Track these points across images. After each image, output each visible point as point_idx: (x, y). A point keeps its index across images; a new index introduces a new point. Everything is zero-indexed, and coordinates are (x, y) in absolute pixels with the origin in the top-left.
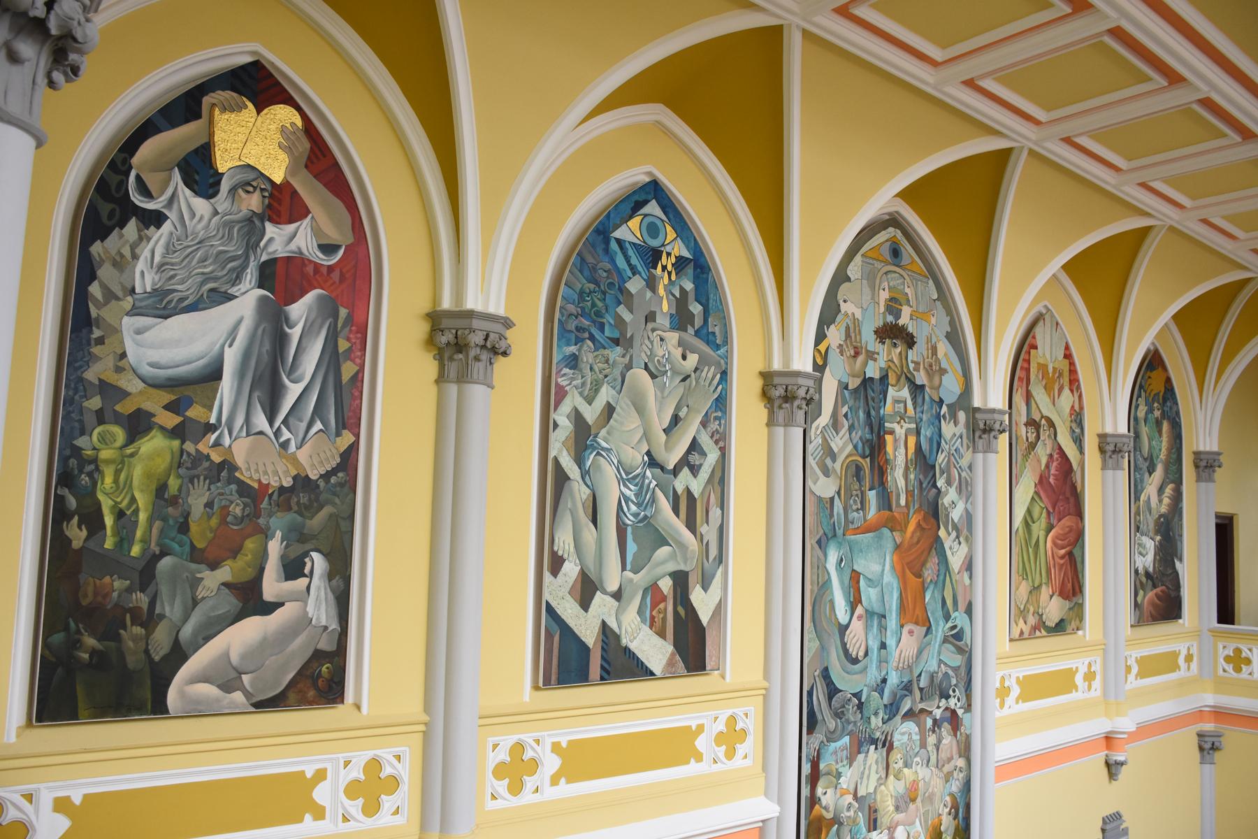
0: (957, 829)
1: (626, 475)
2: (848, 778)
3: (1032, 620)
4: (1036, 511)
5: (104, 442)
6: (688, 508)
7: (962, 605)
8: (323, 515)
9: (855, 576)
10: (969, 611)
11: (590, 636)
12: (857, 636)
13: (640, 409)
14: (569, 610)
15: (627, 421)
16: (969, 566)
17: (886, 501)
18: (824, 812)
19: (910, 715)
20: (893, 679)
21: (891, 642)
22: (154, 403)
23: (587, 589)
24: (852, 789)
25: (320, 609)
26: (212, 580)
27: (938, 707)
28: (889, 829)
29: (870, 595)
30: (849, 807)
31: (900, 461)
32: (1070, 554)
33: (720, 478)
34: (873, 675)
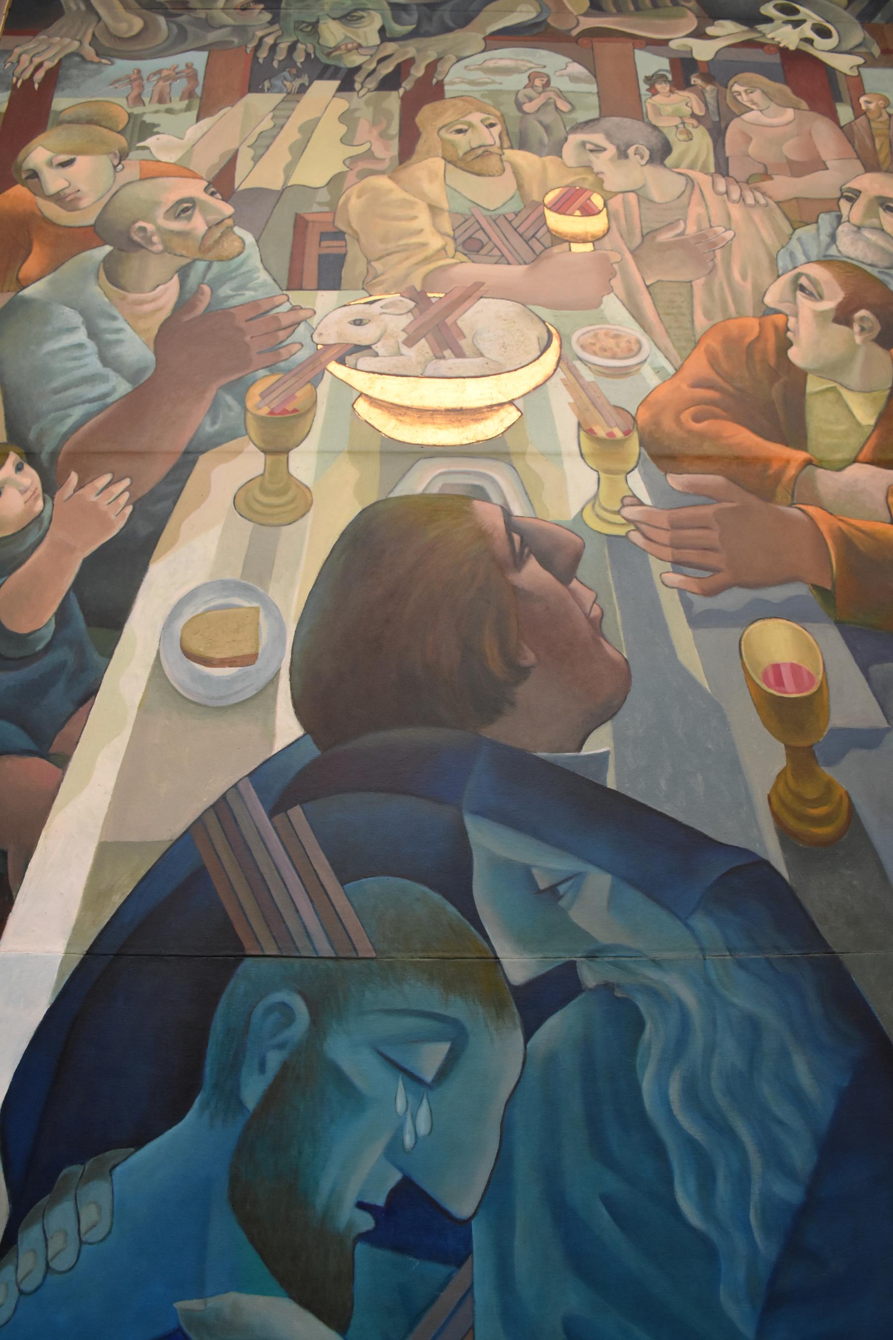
18: (51, 210)
24: (207, 162)
27: (699, 34)
28: (419, 298)
30: (184, 208)
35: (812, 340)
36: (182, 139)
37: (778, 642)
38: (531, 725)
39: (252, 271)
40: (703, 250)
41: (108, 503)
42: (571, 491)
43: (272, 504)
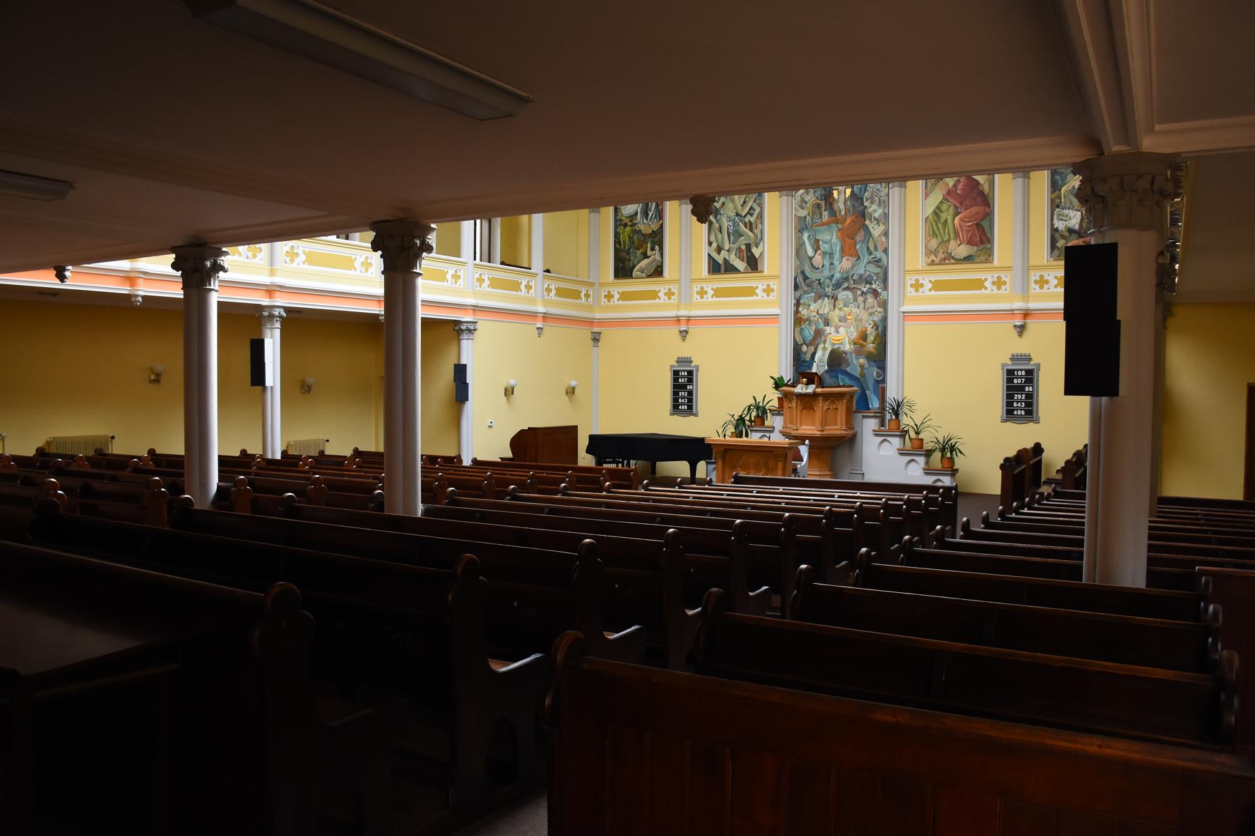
0: (877, 335)
1: (729, 219)
2: (813, 307)
3: (941, 256)
4: (944, 207)
5: (621, 229)
6: (750, 226)
7: (880, 249)
8: (657, 238)
9: (817, 241)
10: (886, 251)
11: (720, 261)
12: (818, 260)
13: (733, 201)
14: (715, 255)
15: (730, 205)
16: (886, 234)
17: (833, 213)
19: (847, 289)
20: (837, 276)
21: (836, 262)
22: (627, 221)
23: (719, 250)
25: (658, 257)
26: (639, 252)
29: (824, 247)
31: (842, 198)
32: (978, 225)
33: (761, 216)
34: (827, 273)
35: (869, 330)
36: (813, 307)
37: (861, 360)
38: (843, 367)
39: (822, 326)
40: (861, 320)
41: (812, 349)
42: (847, 347)
43: (824, 349)
